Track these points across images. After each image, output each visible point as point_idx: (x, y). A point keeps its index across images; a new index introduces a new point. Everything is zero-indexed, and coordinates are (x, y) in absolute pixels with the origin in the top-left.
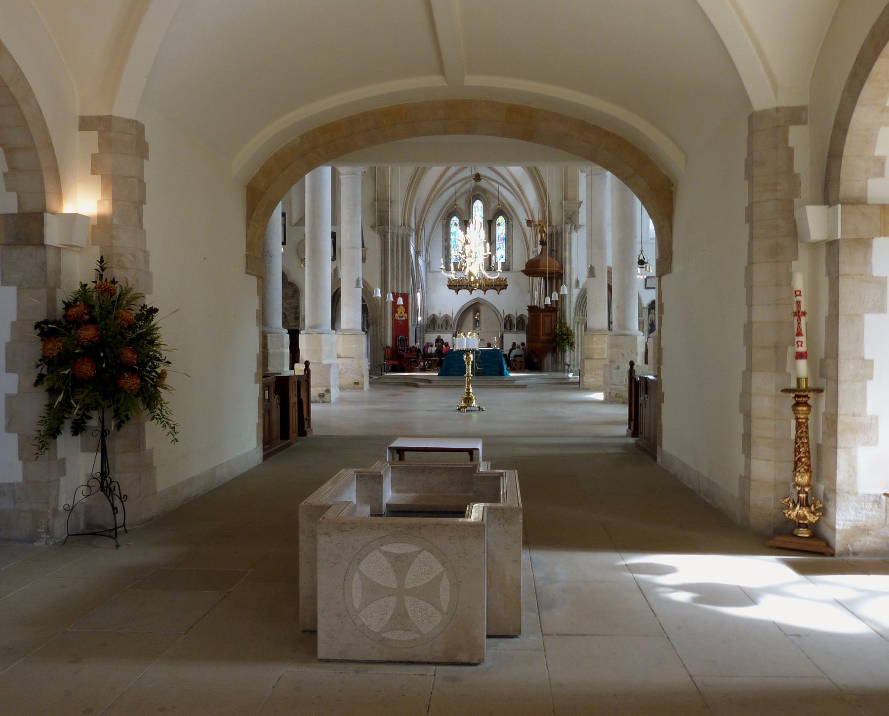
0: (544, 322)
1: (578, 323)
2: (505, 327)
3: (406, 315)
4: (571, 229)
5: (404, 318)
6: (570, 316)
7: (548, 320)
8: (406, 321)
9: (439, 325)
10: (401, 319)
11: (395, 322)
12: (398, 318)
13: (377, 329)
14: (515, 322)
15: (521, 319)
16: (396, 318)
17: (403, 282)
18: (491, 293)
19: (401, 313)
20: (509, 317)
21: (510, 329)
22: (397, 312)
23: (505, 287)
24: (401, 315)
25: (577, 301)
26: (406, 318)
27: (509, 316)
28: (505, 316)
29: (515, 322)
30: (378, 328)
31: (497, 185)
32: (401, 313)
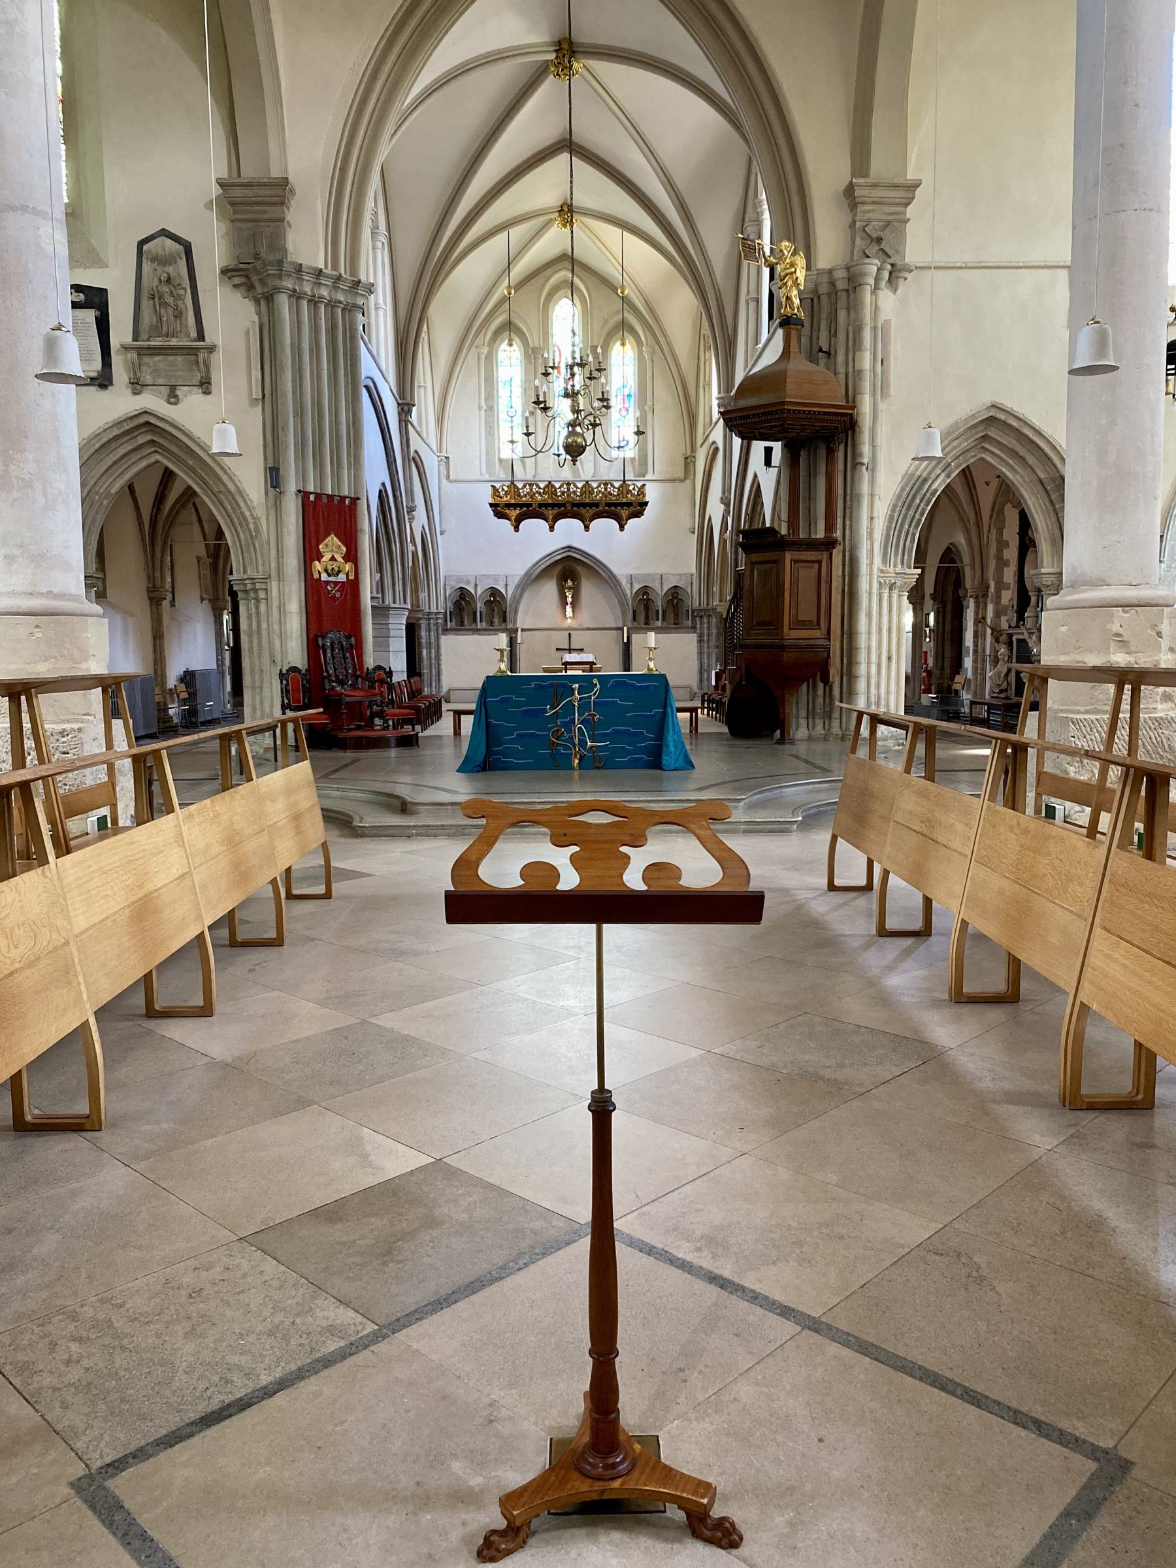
0: (795, 583)
1: (892, 587)
2: (634, 619)
3: (348, 567)
4: (877, 279)
5: (342, 577)
6: (871, 564)
7: (807, 575)
8: (353, 586)
9: (475, 613)
10: (332, 579)
11: (314, 589)
12: (324, 577)
13: (258, 613)
14: (659, 604)
15: (675, 596)
16: (316, 576)
17: (339, 465)
18: (604, 526)
19: (333, 559)
20: (646, 593)
21: (647, 623)
22: (319, 557)
23: (638, 508)
24: (335, 566)
25: (891, 518)
26: (352, 577)
27: (645, 590)
28: (634, 591)
29: (659, 604)
30: (263, 608)
31: (612, 234)
32: (333, 559)
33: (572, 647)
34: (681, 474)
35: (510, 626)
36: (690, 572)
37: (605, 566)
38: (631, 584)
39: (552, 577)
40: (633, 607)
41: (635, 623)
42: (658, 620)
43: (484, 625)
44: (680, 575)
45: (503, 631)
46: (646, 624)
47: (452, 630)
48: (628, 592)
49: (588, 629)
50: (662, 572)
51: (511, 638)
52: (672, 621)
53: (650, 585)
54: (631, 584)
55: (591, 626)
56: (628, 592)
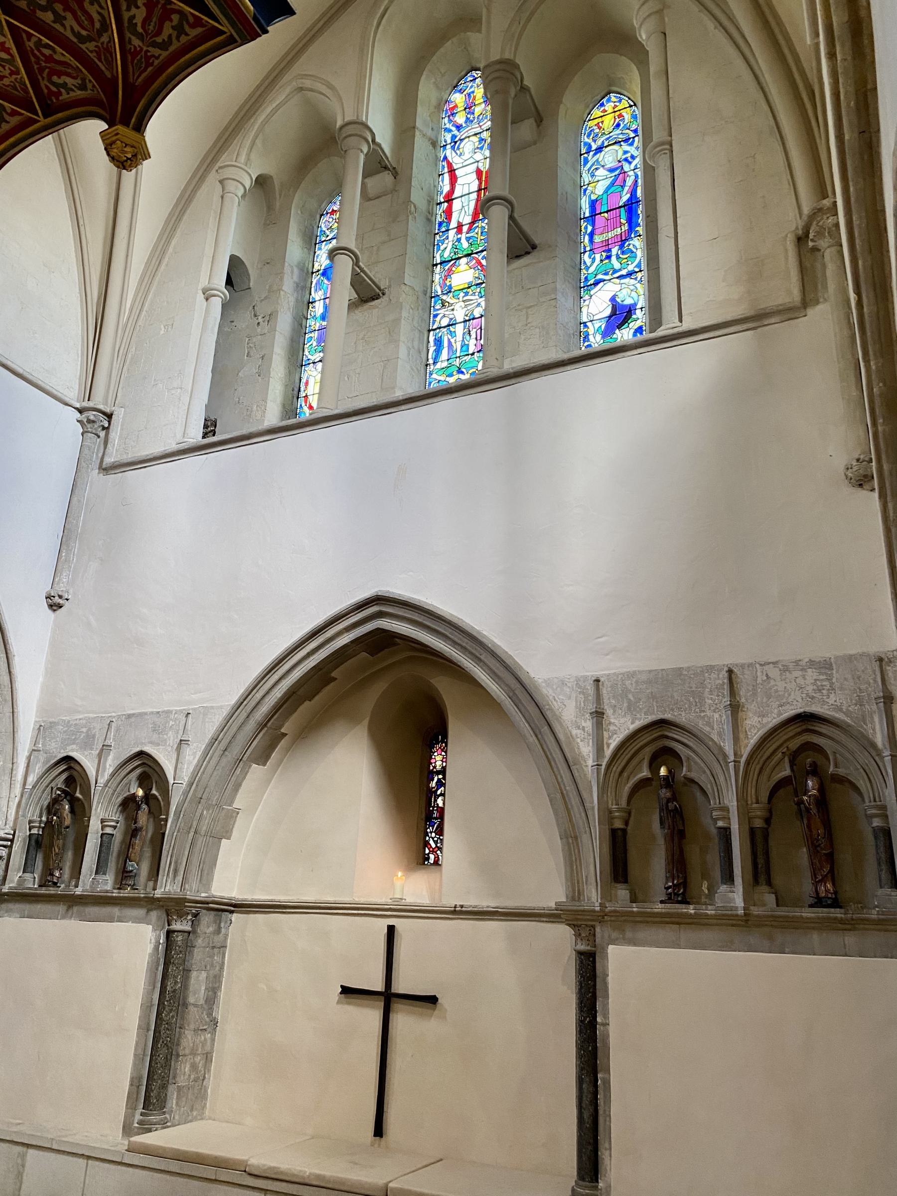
33: (379, 987)
34: (796, 295)
35: (167, 887)
36: (874, 648)
37: (493, 654)
38: (599, 715)
39: (353, 719)
40: (607, 815)
41: (622, 893)
42: (729, 878)
43: (107, 883)
44: (825, 666)
45: (151, 903)
46: (670, 899)
47: (21, 897)
48: (586, 750)
49: (457, 913)
50: (729, 660)
51: (169, 933)
52: (807, 887)
53: (682, 718)
54: (599, 715)
55: (472, 901)
56: (586, 750)
